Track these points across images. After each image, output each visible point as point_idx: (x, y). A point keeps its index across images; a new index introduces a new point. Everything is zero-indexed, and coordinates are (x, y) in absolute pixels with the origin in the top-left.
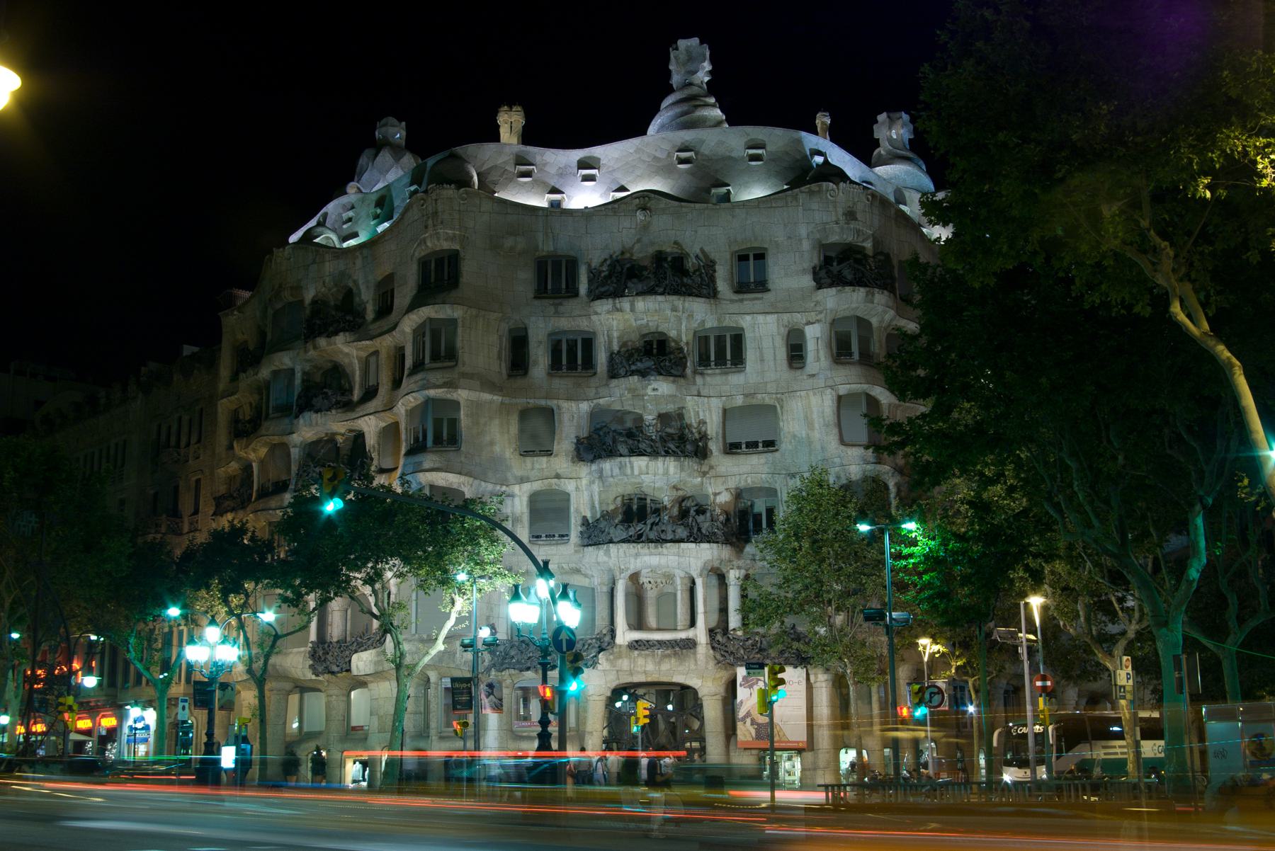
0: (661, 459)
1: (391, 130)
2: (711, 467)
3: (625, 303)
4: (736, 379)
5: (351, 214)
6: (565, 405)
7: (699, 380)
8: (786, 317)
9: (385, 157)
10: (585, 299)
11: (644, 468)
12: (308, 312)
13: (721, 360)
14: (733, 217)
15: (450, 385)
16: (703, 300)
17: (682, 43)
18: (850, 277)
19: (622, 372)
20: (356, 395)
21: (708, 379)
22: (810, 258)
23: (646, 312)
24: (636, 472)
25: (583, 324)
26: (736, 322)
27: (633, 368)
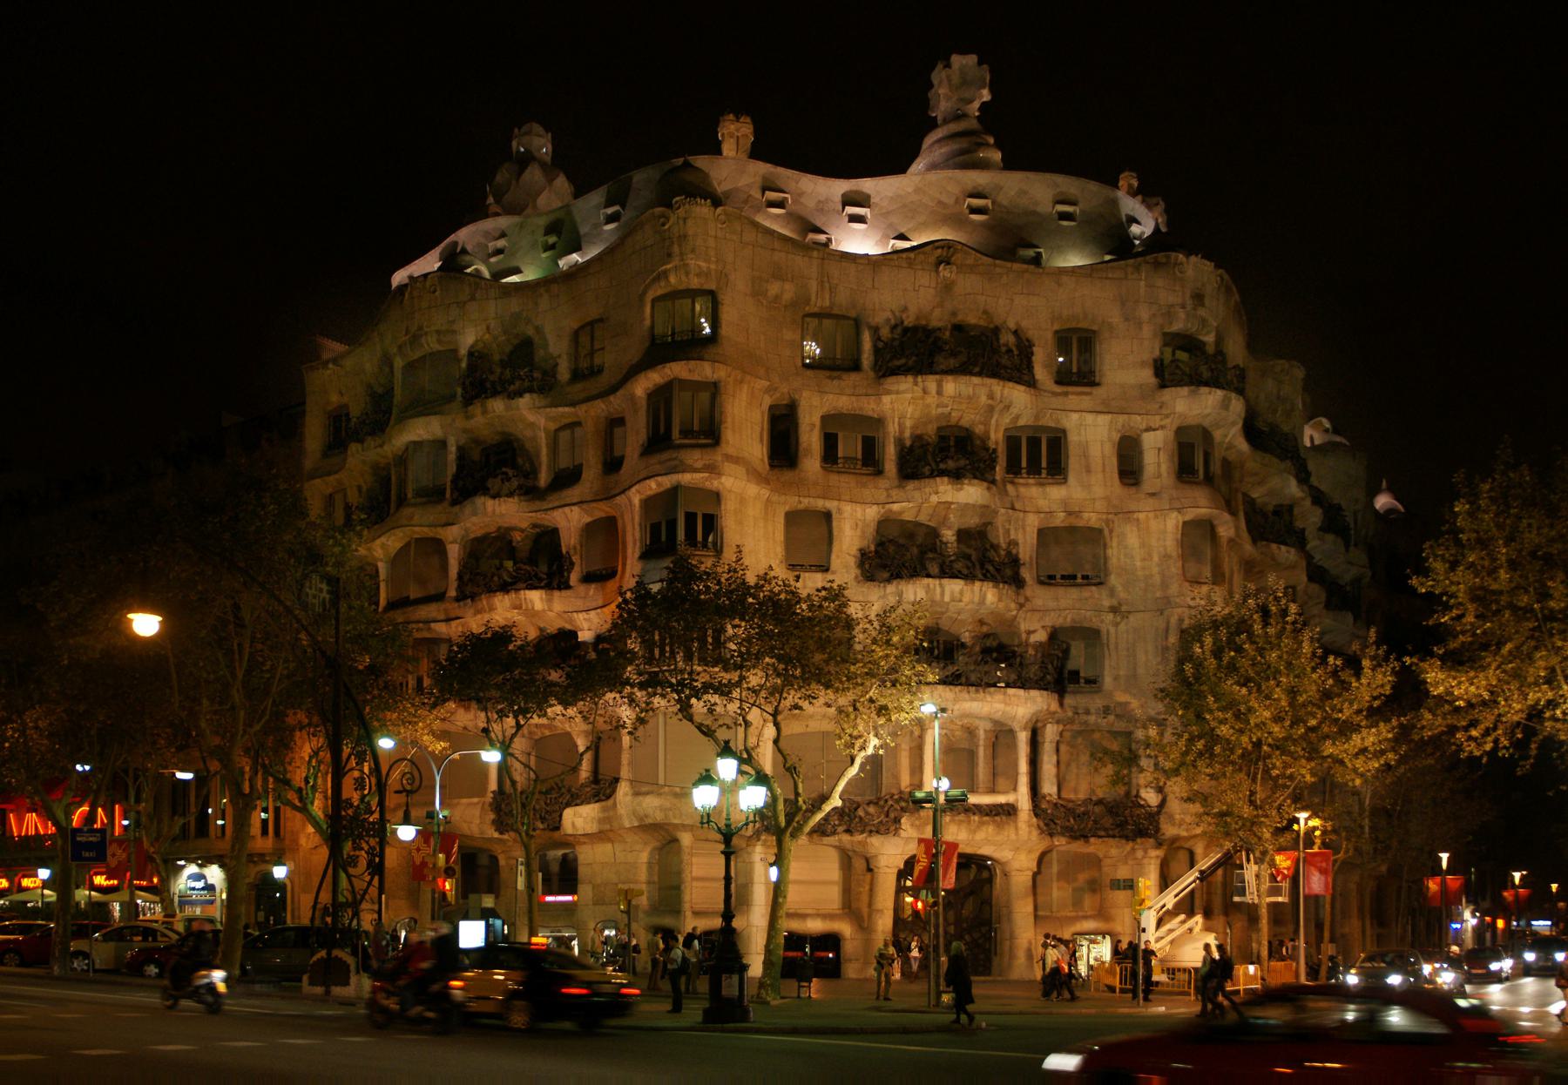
0: (978, 584)
1: (537, 141)
2: (1027, 599)
3: (931, 382)
4: (1056, 493)
5: (501, 243)
6: (847, 508)
7: (1010, 487)
8: (1121, 419)
9: (533, 174)
10: (872, 374)
11: (957, 595)
12: (464, 365)
13: (1034, 469)
14: (1059, 285)
15: (712, 469)
16: (1022, 388)
18: (1206, 374)
19: (927, 470)
20: (544, 479)
21: (1022, 490)
22: (1150, 347)
23: (957, 397)
24: (947, 599)
25: (869, 407)
26: (1058, 421)
27: (942, 466)
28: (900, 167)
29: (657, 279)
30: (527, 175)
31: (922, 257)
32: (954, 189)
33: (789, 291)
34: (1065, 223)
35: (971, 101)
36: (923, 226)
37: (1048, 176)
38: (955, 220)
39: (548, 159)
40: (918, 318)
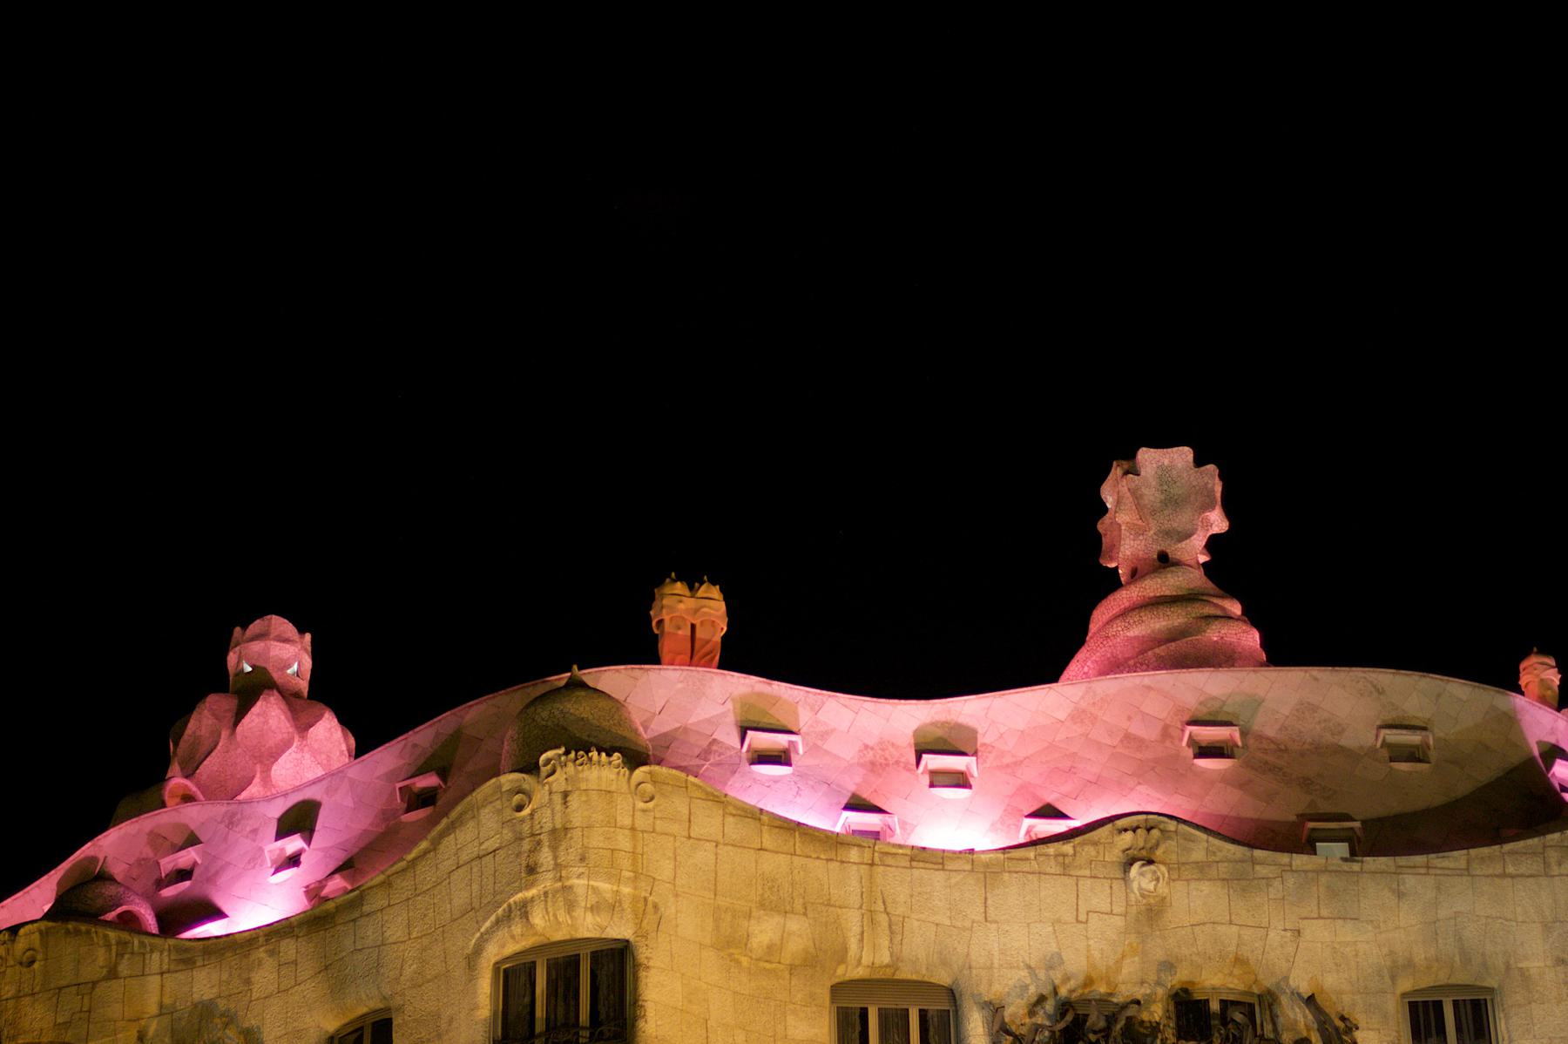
1: (279, 651)
9: (268, 716)
14: (1400, 895)
17: (1148, 457)
28: (1044, 668)
29: (508, 917)
30: (252, 720)
31: (1090, 851)
32: (1157, 708)
33: (798, 933)
34: (1404, 767)
35: (1188, 536)
36: (1097, 785)
37: (1358, 673)
38: (1163, 770)
39: (304, 685)
40: (1089, 982)
